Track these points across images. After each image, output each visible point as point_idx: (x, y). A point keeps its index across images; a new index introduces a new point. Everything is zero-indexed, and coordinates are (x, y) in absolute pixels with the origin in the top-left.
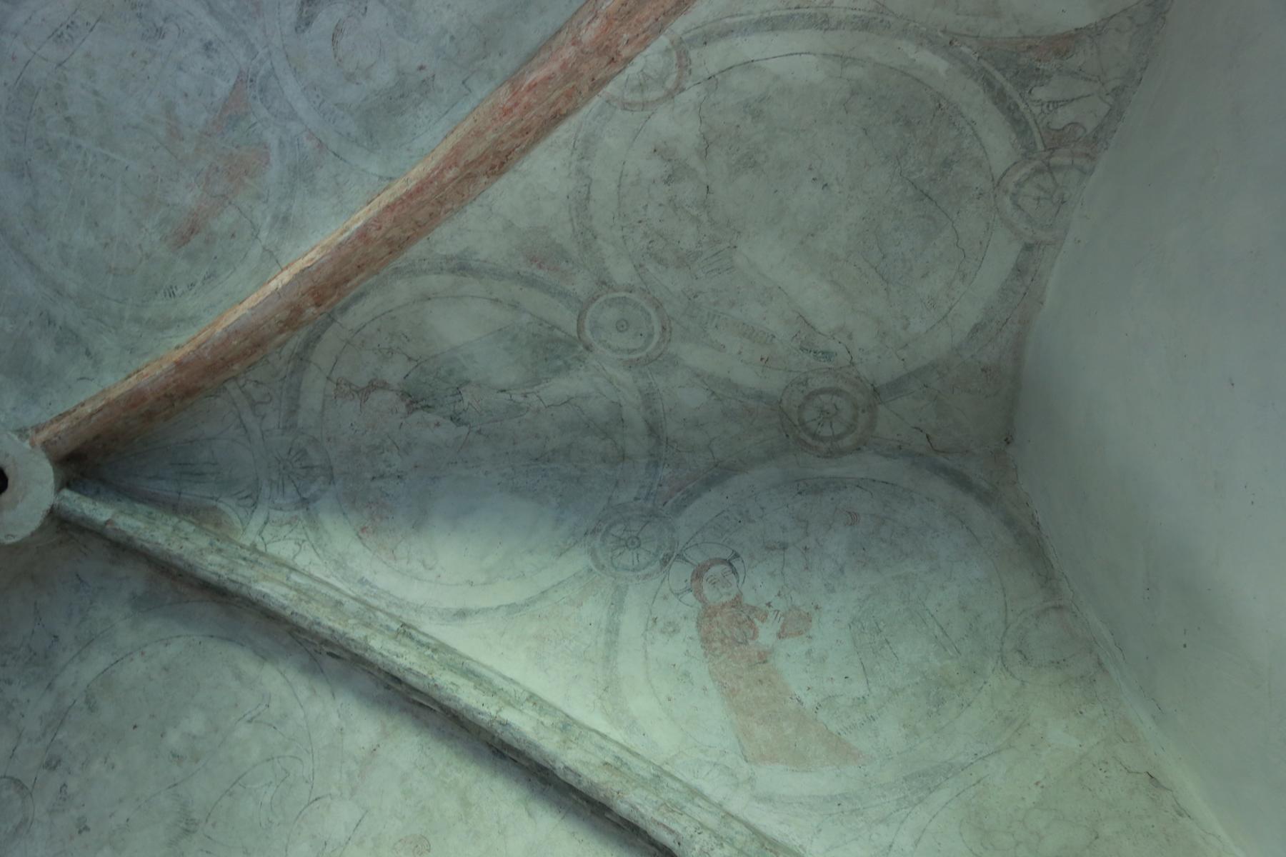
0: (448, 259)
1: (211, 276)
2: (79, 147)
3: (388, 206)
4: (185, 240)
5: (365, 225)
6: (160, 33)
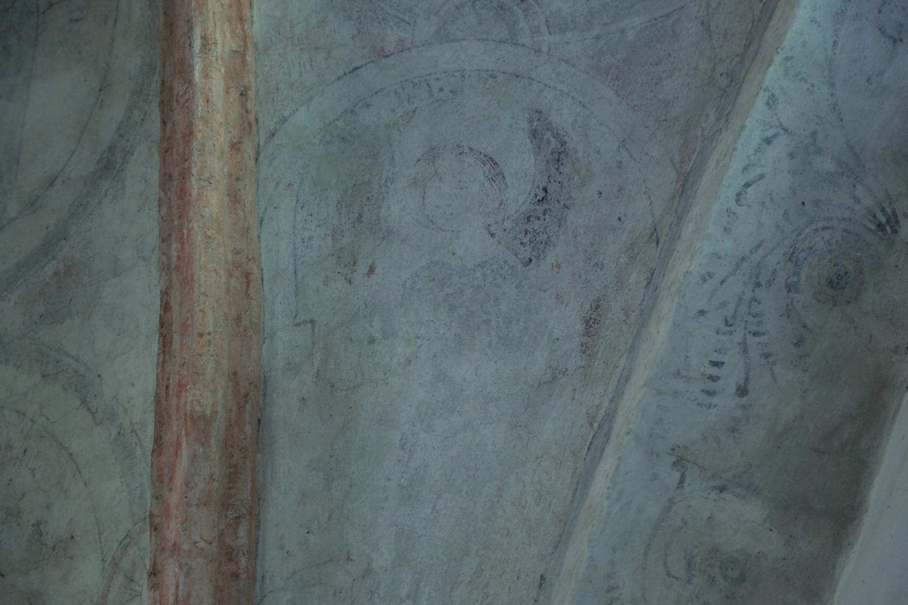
0: (128, 153)
3: (191, 133)
5: (190, 82)
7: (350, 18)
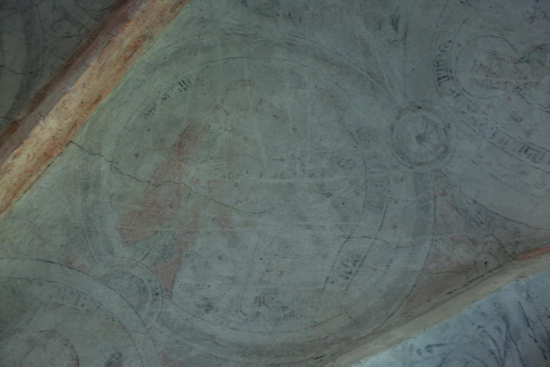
1: (149, 112)
2: (312, 175)
4: (185, 135)
6: (260, 301)
7: (68, 236)
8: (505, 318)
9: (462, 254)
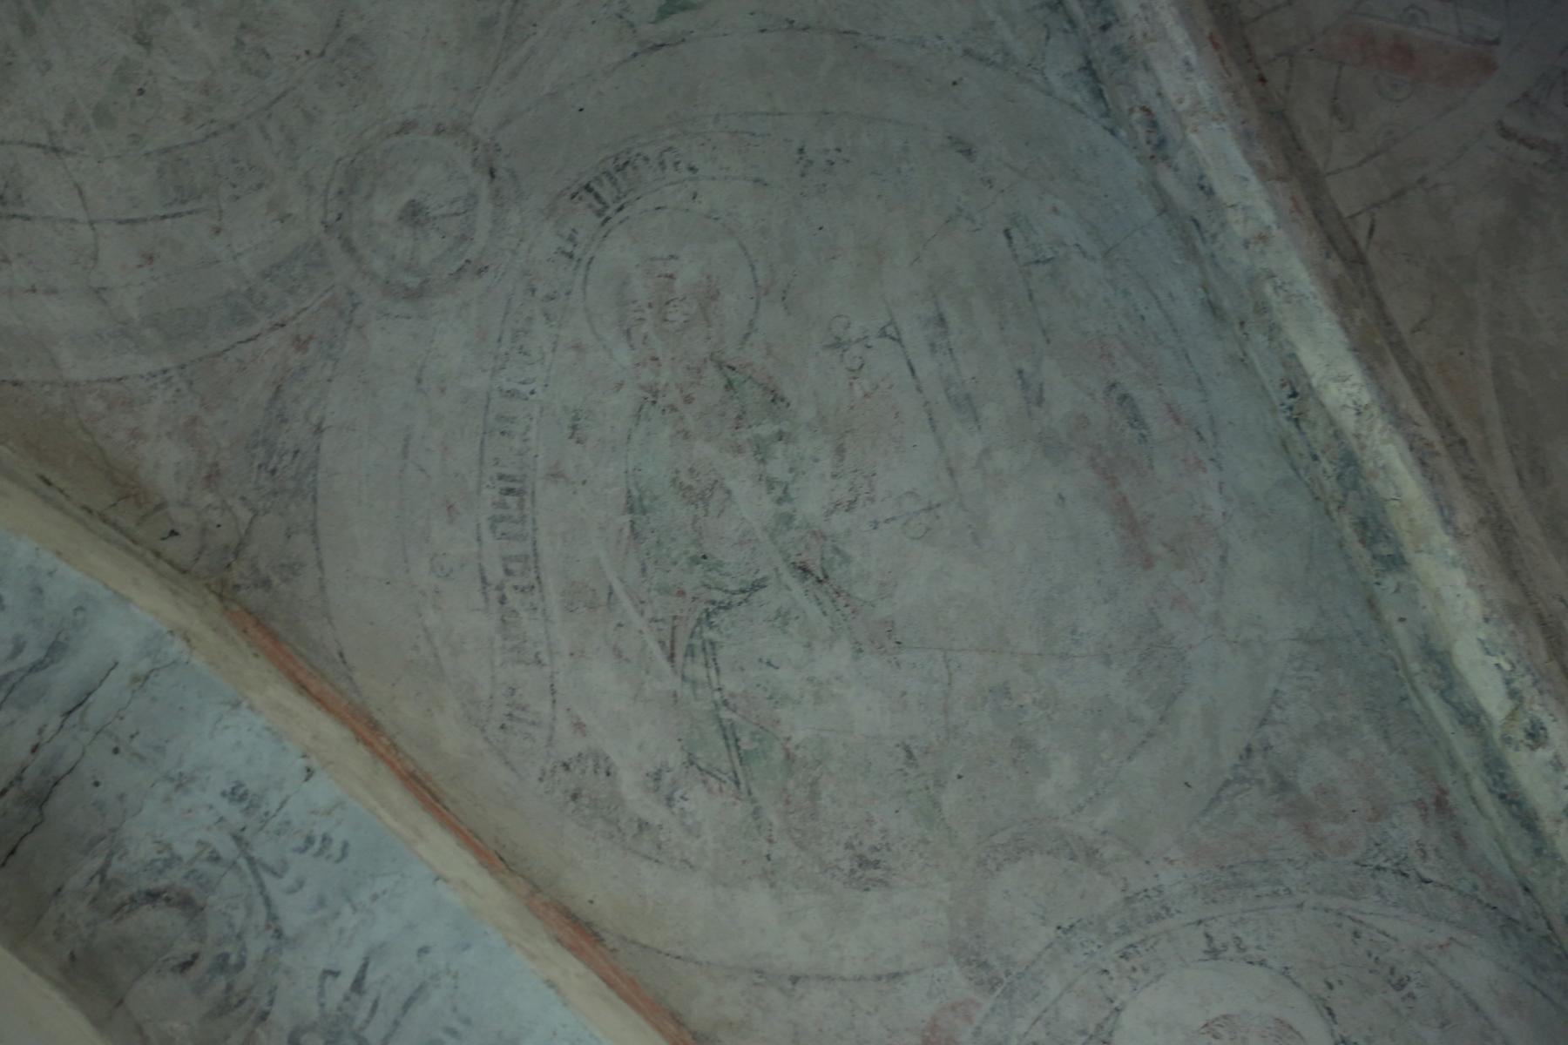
8: (56, 650)
9: (165, 463)
